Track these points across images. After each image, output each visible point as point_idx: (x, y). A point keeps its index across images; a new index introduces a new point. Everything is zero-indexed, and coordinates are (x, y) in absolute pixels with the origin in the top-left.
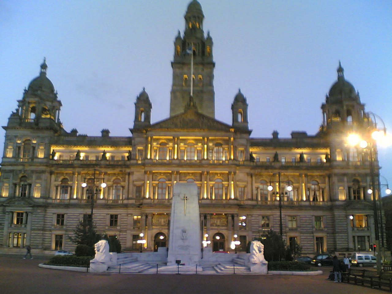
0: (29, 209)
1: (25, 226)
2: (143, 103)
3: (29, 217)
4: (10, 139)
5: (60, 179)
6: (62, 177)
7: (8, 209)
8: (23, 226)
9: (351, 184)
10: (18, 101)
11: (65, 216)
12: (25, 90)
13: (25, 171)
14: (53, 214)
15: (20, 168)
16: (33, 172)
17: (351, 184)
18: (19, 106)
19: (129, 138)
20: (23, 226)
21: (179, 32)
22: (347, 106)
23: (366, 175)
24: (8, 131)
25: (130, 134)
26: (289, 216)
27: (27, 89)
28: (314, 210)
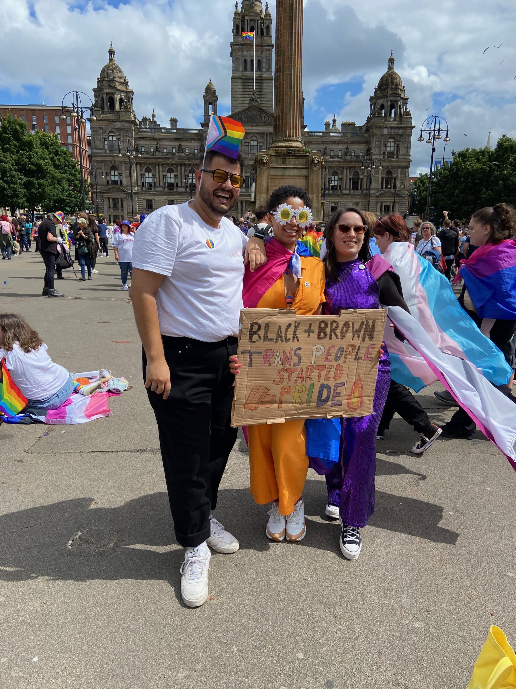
0: (123, 195)
1: (122, 210)
2: (210, 97)
3: (125, 203)
4: (96, 132)
5: (144, 169)
6: (146, 167)
7: (106, 196)
8: (120, 210)
9: (384, 176)
10: (94, 90)
11: (153, 201)
12: (98, 79)
13: (115, 161)
14: (143, 199)
15: (110, 159)
16: (121, 162)
17: (384, 176)
18: (96, 96)
19: (199, 130)
20: (120, 210)
21: (237, 2)
22: (391, 101)
23: (398, 167)
24: (92, 124)
25: (200, 128)
26: (332, 202)
27: (99, 77)
28: (352, 198)
